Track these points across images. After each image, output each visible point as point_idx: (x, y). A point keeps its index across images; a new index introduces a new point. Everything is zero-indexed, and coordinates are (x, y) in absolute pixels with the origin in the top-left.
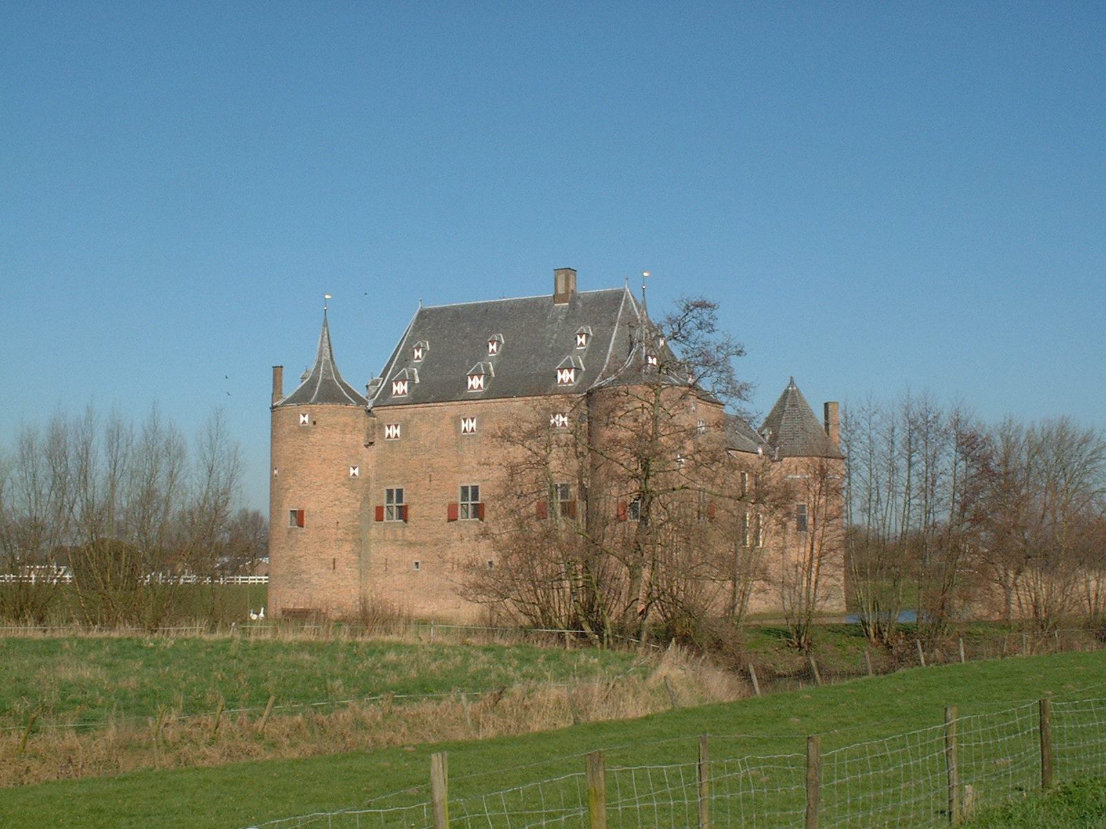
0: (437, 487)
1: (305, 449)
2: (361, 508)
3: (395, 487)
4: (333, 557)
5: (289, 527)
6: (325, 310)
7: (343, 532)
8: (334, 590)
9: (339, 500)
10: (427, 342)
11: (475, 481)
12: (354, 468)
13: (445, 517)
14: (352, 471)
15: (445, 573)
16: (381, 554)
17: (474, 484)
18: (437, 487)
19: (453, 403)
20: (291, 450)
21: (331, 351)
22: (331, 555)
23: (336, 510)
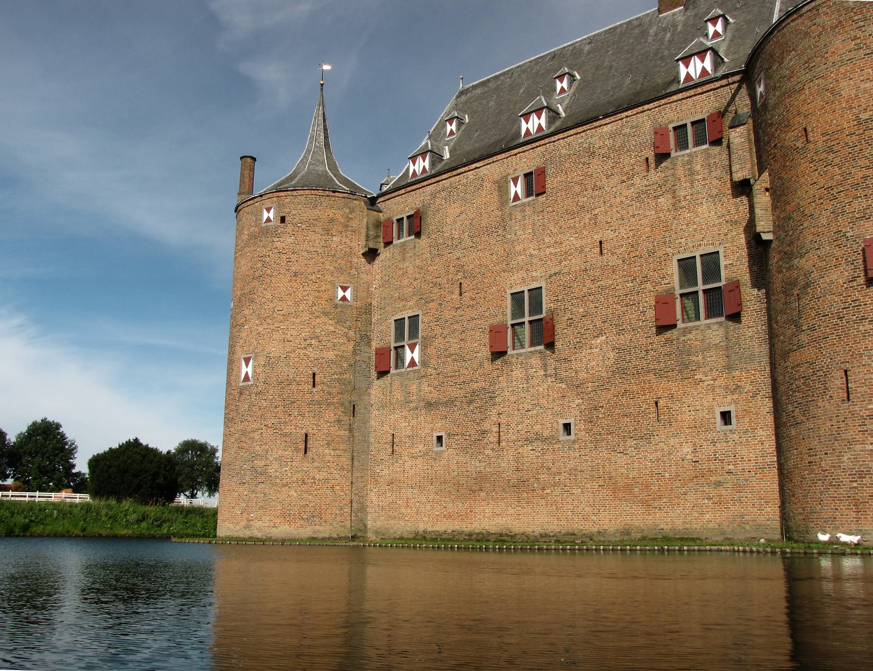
0: (471, 303)
1: (268, 259)
2: (354, 352)
3: (406, 315)
4: (304, 431)
5: (242, 384)
6: (322, 85)
7: (323, 390)
8: (305, 487)
9: (318, 337)
10: (467, 116)
11: (534, 279)
12: (344, 289)
13: (486, 352)
14: (340, 293)
15: (486, 452)
16: (386, 428)
19: (495, 158)
20: (249, 265)
21: (326, 137)
22: (302, 428)
23: (312, 353)
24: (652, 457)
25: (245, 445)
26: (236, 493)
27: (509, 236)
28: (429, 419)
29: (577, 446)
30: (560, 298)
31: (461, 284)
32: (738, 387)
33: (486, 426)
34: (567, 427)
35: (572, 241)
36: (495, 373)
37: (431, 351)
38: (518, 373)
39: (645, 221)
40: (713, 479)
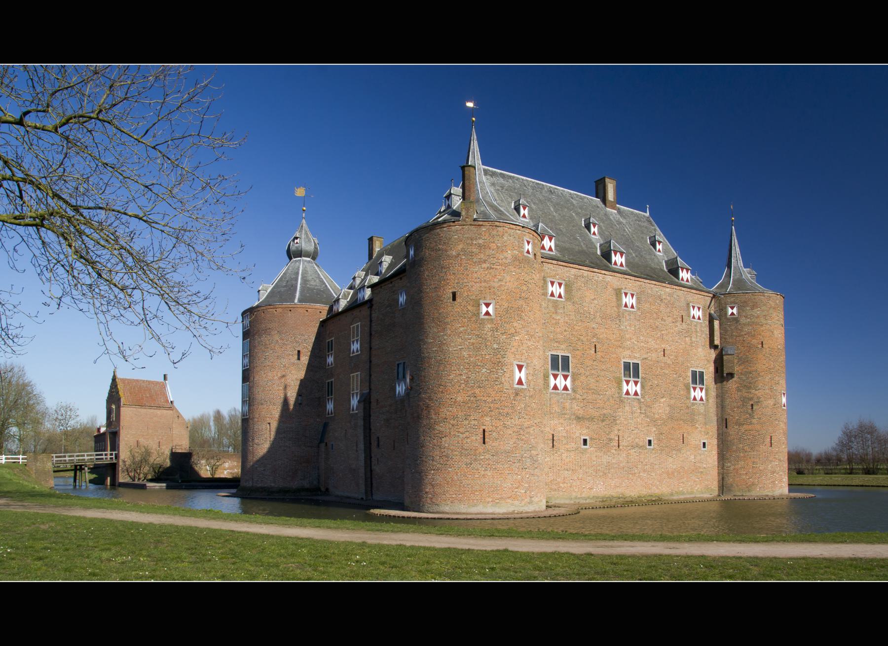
0: (602, 360)
3: (560, 353)
17: (636, 361)
18: (602, 360)
24: (681, 459)
25: (524, 437)
26: (519, 477)
27: (622, 327)
28: (578, 427)
29: (654, 452)
30: (647, 372)
31: (595, 345)
32: (708, 433)
33: (612, 436)
34: (650, 442)
35: (652, 343)
36: (616, 406)
37: (578, 383)
38: (627, 408)
39: (681, 346)
40: (700, 470)
